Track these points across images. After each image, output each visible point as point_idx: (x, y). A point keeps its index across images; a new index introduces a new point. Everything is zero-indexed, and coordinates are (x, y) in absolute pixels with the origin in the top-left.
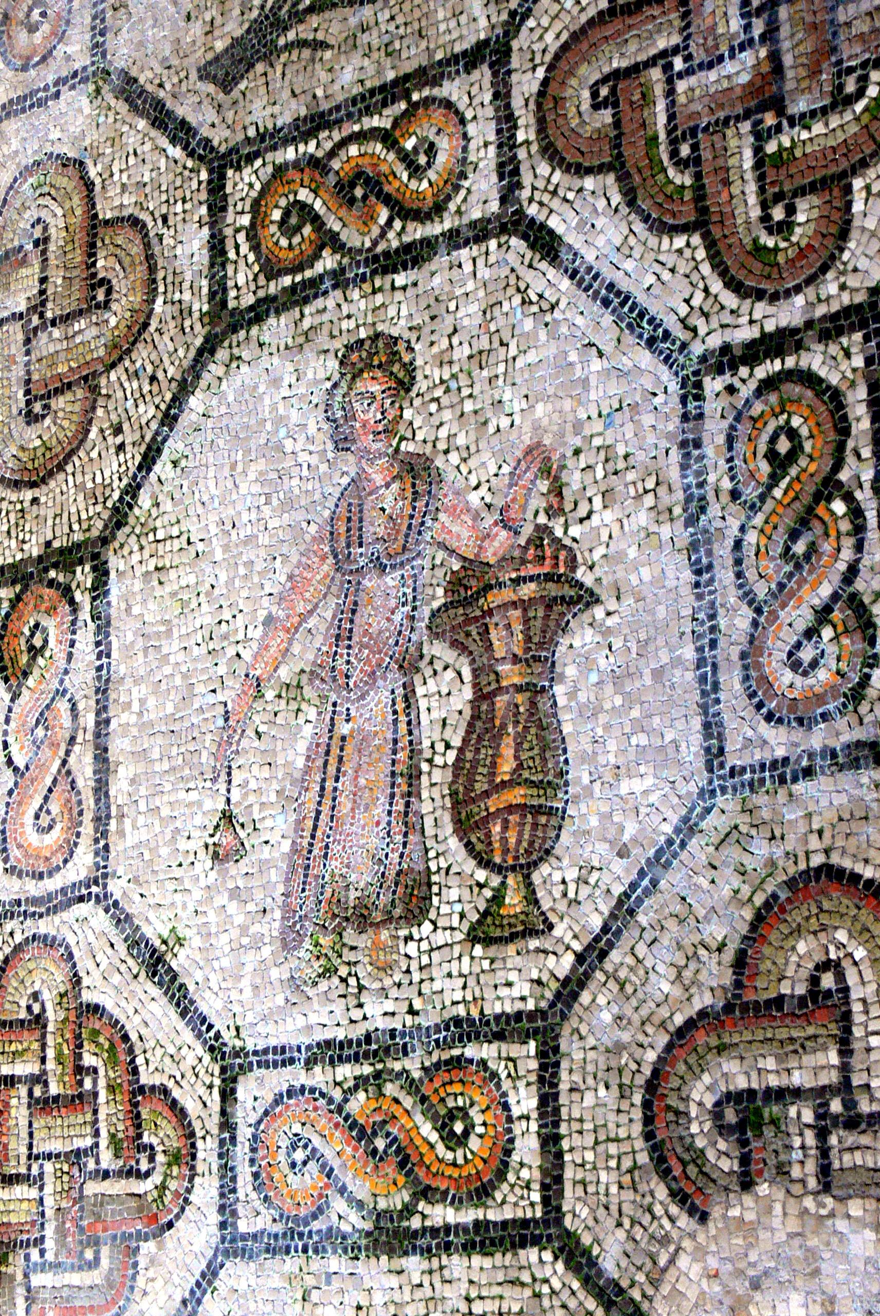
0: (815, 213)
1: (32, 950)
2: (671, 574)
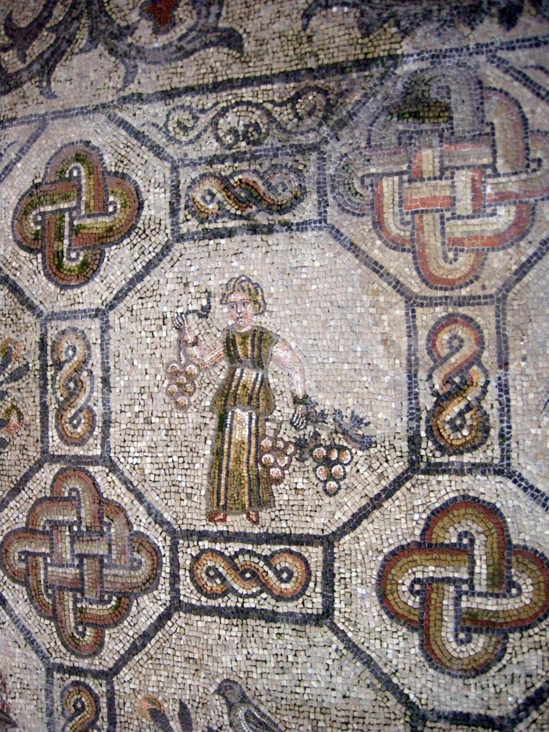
0: (92, 634)
2: (41, 728)
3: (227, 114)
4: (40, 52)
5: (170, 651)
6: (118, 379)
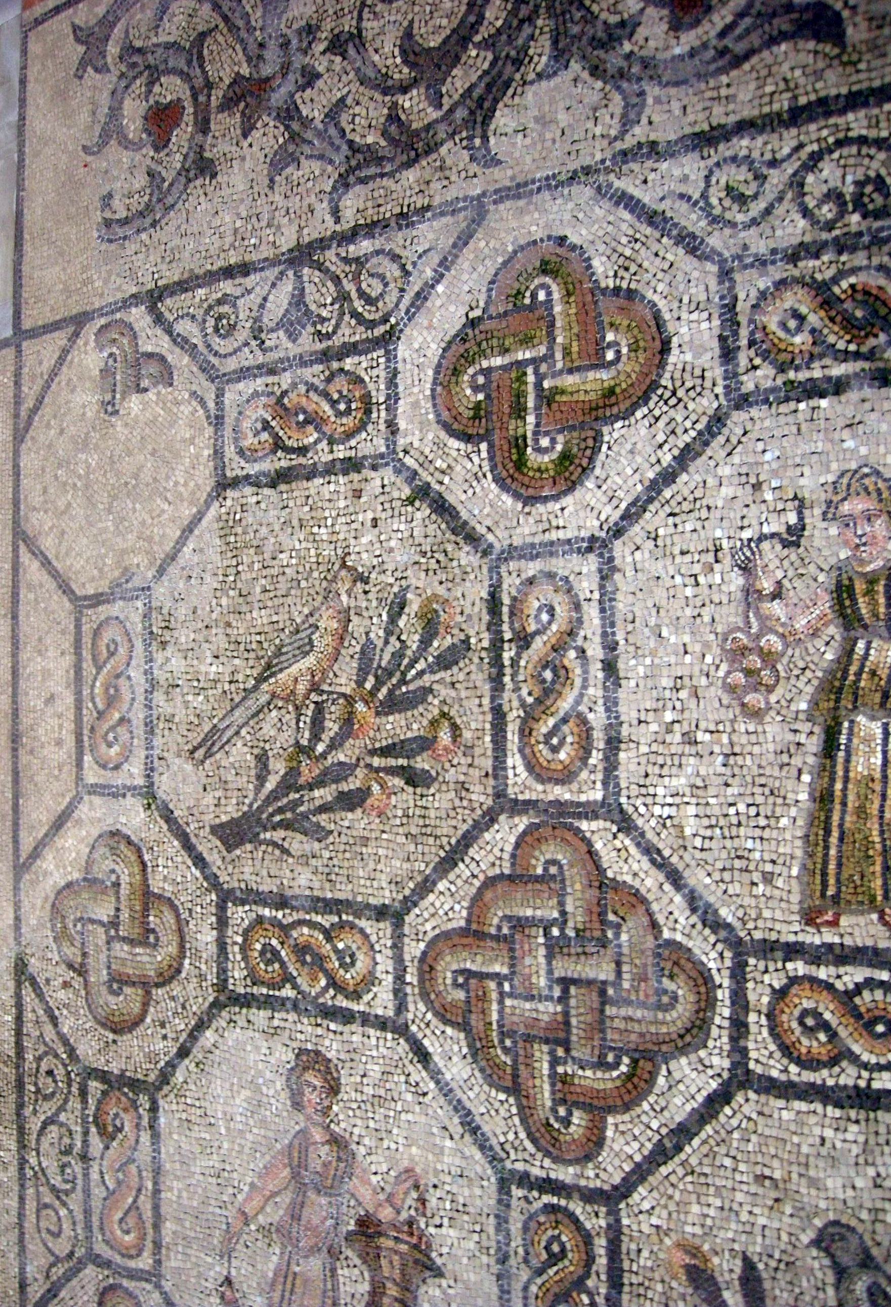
0: (583, 1123)
1: (119, 1292)
2: (486, 1284)
3: (820, 165)
4: (466, 86)
5: (728, 1162)
6: (633, 662)
